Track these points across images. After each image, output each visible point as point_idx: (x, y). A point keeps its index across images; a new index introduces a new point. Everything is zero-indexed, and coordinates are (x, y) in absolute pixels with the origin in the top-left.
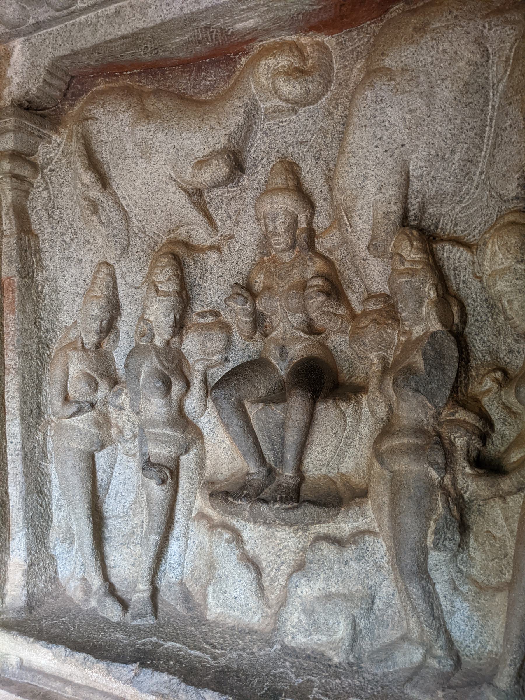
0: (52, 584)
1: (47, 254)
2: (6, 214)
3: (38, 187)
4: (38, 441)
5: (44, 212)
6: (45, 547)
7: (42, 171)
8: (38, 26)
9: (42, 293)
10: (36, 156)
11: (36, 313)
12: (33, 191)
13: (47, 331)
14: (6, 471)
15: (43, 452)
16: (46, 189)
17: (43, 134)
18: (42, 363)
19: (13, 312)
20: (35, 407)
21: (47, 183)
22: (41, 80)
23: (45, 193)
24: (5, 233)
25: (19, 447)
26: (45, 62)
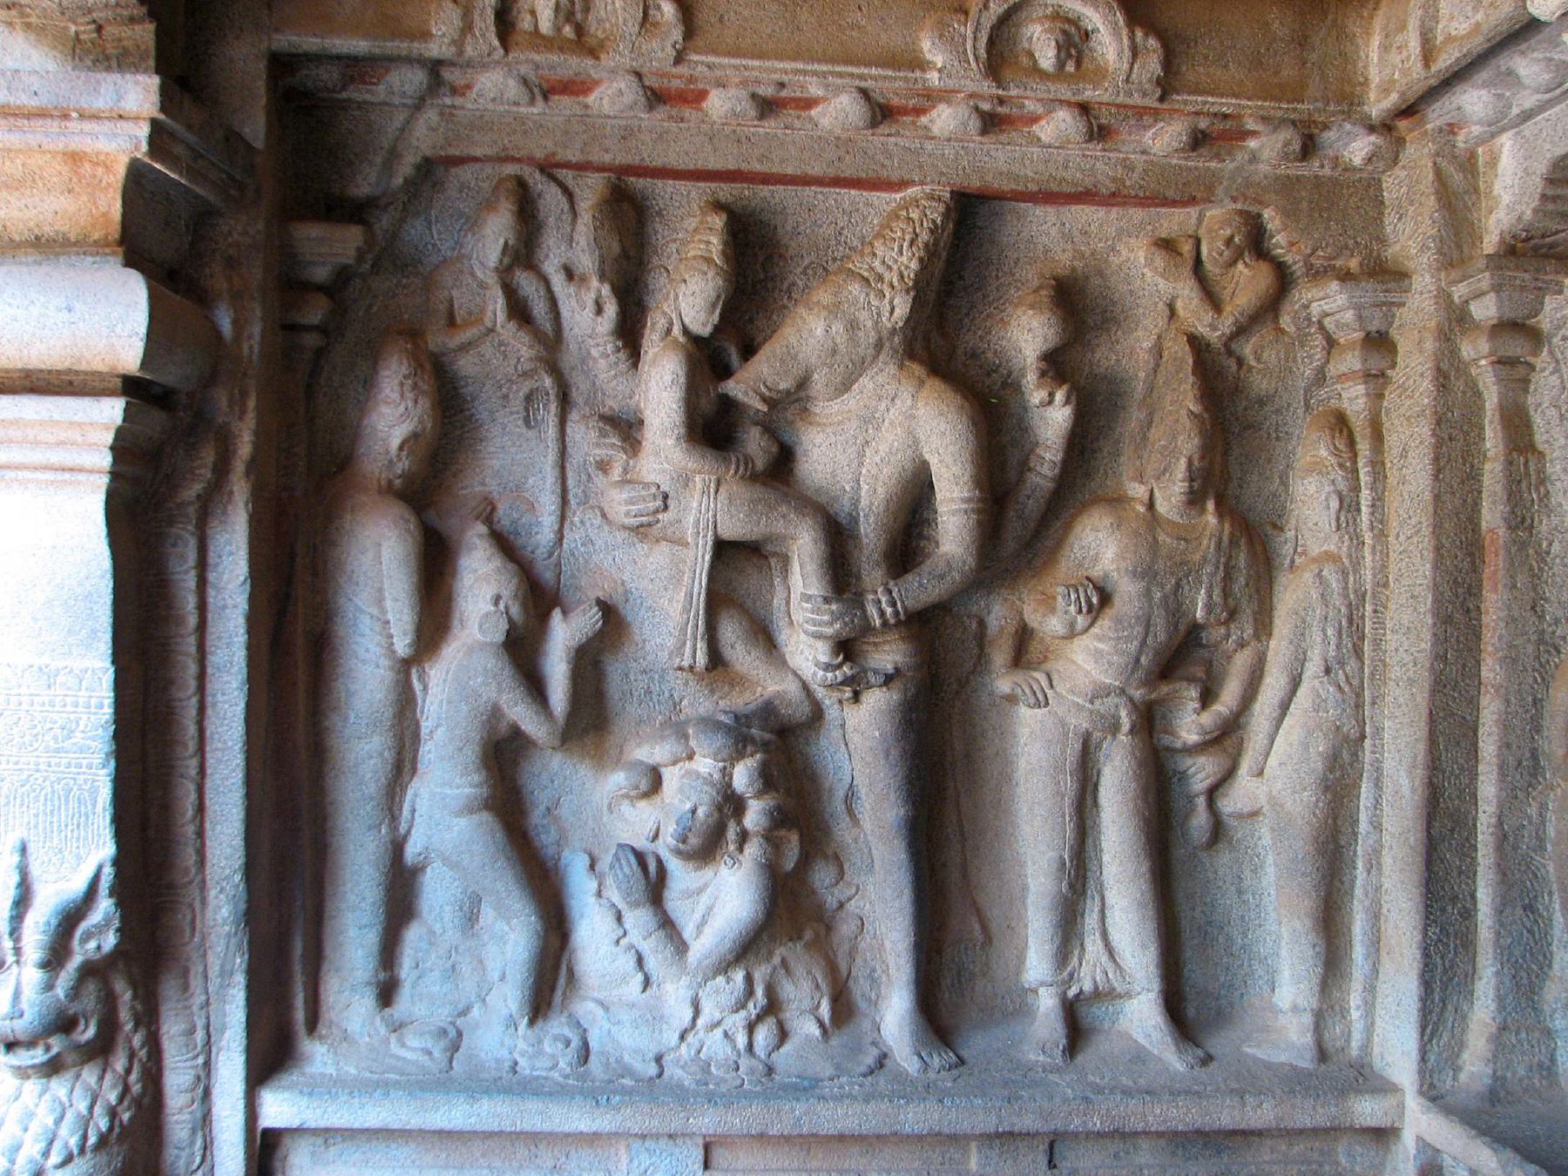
0: (1542, 1077)
1: (1558, 484)
2: (1491, 422)
3: (1543, 370)
4: (1530, 818)
5: (1553, 412)
6: (1534, 1009)
7: (1550, 343)
8: (1527, 116)
9: (1548, 553)
10: (1540, 317)
11: (1535, 589)
12: (1534, 377)
13: (1557, 622)
14: (1474, 859)
15: (1538, 838)
16: (1556, 371)
17: (1544, 282)
18: (1543, 679)
19: (1495, 590)
20: (1528, 755)
21: (1557, 361)
22: (1537, 196)
23: (1554, 378)
24: (1489, 454)
25: (1494, 820)
26: (1541, 167)
